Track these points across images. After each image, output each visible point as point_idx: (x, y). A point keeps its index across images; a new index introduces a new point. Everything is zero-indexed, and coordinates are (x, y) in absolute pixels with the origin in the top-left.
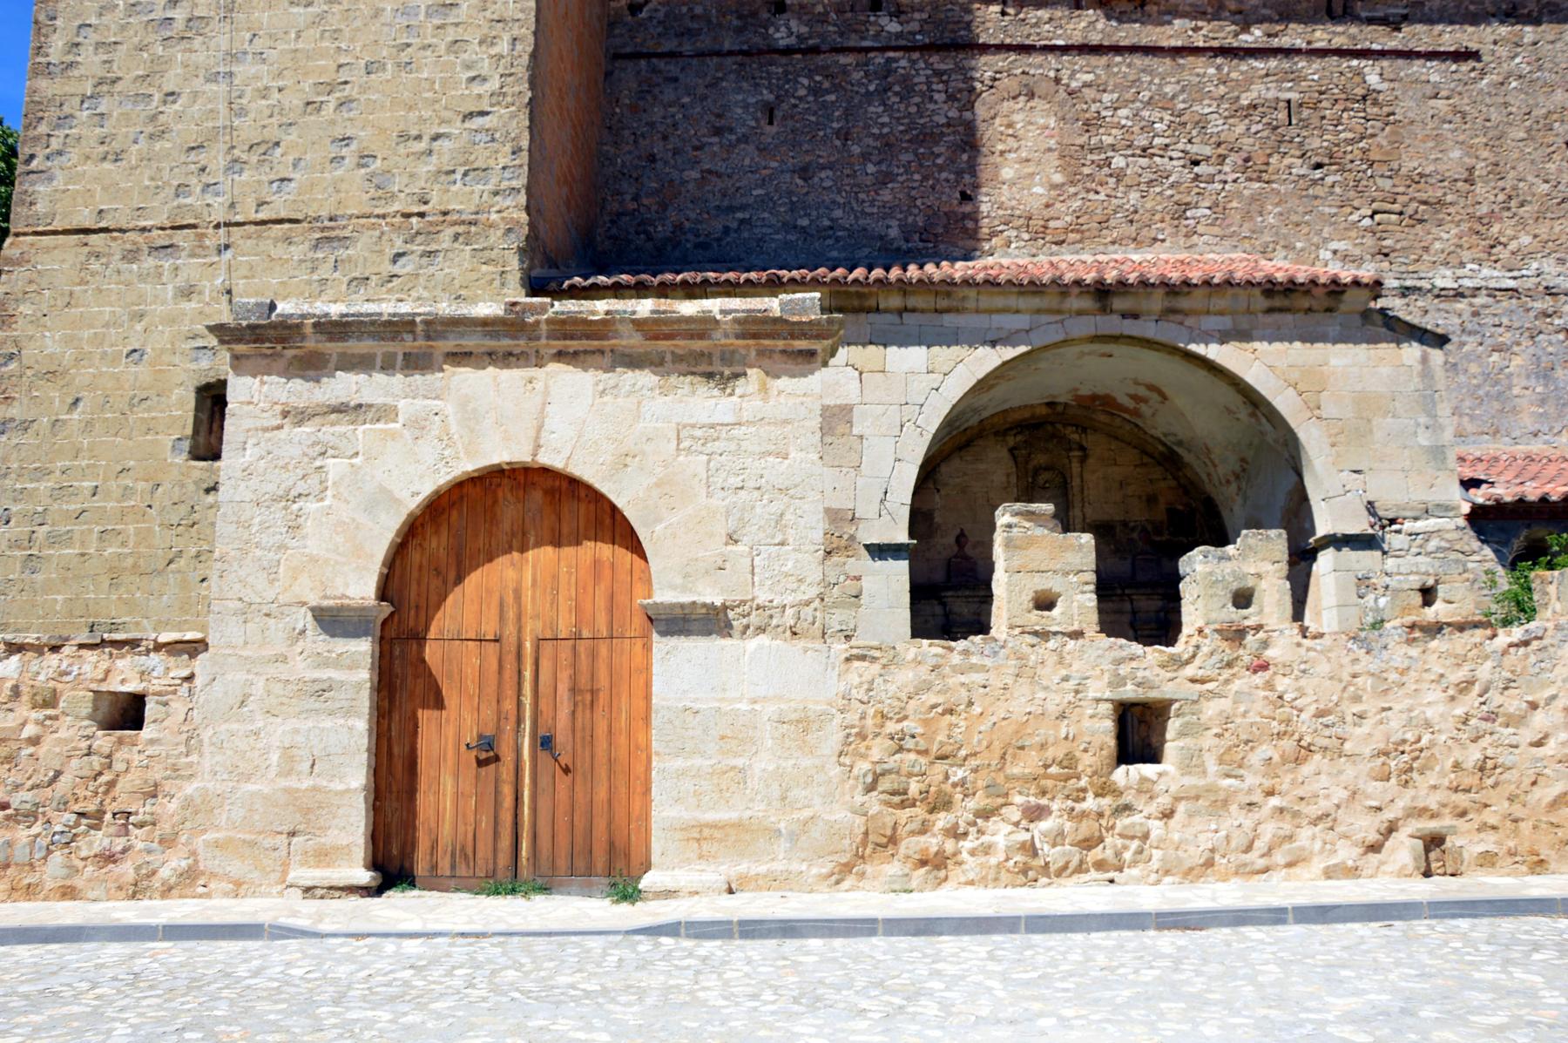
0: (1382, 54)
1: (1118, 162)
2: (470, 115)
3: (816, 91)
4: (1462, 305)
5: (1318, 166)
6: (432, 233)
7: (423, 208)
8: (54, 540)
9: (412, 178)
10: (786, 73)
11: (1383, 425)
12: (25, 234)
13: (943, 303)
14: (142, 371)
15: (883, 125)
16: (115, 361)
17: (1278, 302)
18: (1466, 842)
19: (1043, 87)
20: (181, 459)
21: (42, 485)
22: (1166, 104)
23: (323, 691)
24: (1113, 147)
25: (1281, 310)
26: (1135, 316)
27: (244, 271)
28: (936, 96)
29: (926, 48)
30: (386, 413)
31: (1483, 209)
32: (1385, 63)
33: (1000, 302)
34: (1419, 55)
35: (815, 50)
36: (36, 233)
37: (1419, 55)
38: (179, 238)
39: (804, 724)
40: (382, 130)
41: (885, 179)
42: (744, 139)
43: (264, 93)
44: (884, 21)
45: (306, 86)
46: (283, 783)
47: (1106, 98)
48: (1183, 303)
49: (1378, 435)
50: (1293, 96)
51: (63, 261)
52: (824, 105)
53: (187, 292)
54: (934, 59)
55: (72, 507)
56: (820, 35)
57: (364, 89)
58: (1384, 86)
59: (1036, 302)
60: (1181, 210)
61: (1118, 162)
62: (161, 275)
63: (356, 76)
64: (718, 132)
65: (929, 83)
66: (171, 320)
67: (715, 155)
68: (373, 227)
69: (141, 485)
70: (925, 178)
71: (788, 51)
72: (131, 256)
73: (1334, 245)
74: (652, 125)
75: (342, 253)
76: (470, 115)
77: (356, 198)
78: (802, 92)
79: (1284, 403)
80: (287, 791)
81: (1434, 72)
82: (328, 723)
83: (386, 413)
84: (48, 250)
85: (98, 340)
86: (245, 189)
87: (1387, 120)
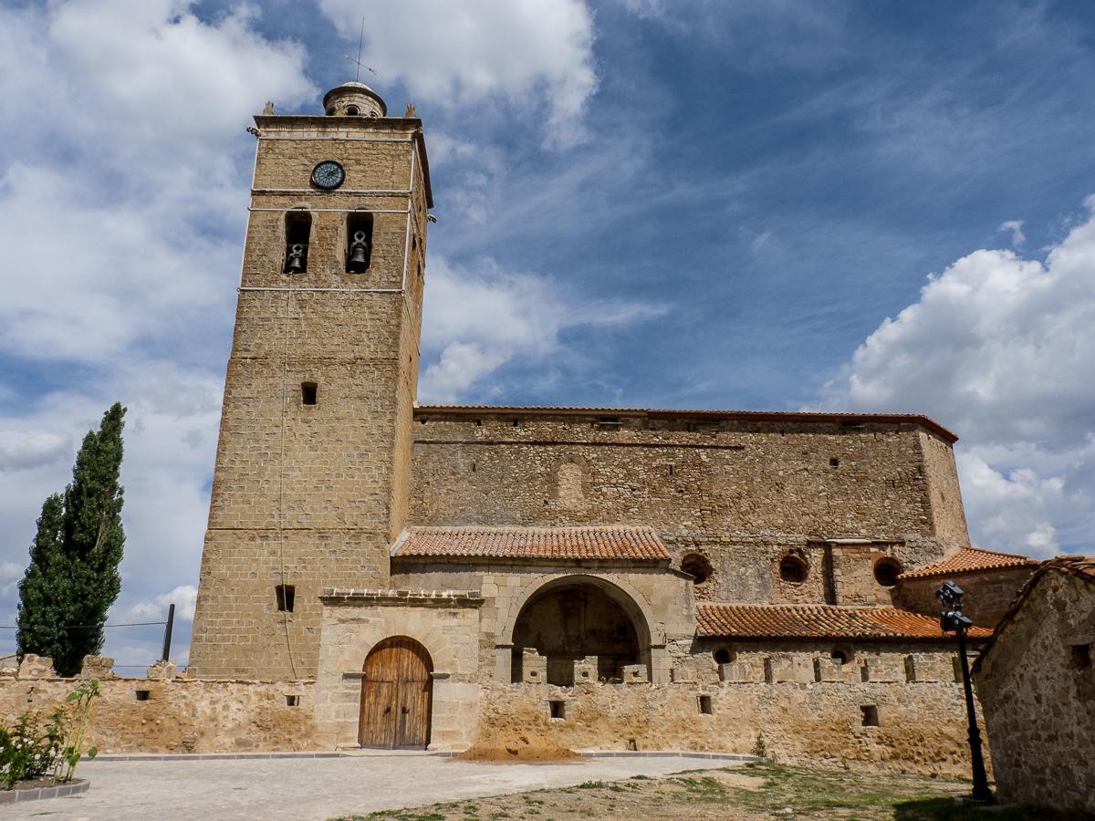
0: (708, 447)
1: (604, 490)
2: (372, 494)
3: (491, 459)
4: (731, 548)
5: (681, 491)
6: (356, 536)
7: (355, 527)
8: (224, 639)
10: (480, 450)
11: (671, 607)
13: (526, 563)
15: (517, 473)
17: (637, 565)
18: (639, 742)
21: (218, 620)
22: (624, 466)
23: (348, 695)
24: (603, 484)
25: (639, 567)
26: (589, 568)
28: (537, 462)
29: (535, 443)
30: (367, 621)
31: (743, 509)
32: (708, 450)
33: (545, 563)
34: (722, 448)
35: (491, 443)
37: (722, 448)
39: (471, 705)
41: (516, 494)
42: (463, 478)
43: (299, 482)
44: (518, 431)
45: (314, 480)
46: (337, 720)
48: (605, 565)
49: (669, 611)
50: (673, 463)
52: (495, 464)
53: (273, 553)
56: (495, 436)
59: (556, 564)
60: (626, 509)
61: (604, 490)
63: (334, 479)
64: (453, 474)
65: (534, 456)
66: (266, 562)
67: (452, 483)
68: (338, 533)
69: (254, 621)
70: (531, 495)
71: (481, 443)
72: (253, 539)
73: (685, 523)
74: (428, 470)
75: (327, 542)
76: (372, 494)
77: (334, 523)
78: (486, 458)
79: (638, 599)
80: (338, 722)
81: (726, 454)
82: (349, 704)
83: (367, 621)
84: (221, 536)
85: (239, 569)
86: (291, 517)
87: (709, 473)
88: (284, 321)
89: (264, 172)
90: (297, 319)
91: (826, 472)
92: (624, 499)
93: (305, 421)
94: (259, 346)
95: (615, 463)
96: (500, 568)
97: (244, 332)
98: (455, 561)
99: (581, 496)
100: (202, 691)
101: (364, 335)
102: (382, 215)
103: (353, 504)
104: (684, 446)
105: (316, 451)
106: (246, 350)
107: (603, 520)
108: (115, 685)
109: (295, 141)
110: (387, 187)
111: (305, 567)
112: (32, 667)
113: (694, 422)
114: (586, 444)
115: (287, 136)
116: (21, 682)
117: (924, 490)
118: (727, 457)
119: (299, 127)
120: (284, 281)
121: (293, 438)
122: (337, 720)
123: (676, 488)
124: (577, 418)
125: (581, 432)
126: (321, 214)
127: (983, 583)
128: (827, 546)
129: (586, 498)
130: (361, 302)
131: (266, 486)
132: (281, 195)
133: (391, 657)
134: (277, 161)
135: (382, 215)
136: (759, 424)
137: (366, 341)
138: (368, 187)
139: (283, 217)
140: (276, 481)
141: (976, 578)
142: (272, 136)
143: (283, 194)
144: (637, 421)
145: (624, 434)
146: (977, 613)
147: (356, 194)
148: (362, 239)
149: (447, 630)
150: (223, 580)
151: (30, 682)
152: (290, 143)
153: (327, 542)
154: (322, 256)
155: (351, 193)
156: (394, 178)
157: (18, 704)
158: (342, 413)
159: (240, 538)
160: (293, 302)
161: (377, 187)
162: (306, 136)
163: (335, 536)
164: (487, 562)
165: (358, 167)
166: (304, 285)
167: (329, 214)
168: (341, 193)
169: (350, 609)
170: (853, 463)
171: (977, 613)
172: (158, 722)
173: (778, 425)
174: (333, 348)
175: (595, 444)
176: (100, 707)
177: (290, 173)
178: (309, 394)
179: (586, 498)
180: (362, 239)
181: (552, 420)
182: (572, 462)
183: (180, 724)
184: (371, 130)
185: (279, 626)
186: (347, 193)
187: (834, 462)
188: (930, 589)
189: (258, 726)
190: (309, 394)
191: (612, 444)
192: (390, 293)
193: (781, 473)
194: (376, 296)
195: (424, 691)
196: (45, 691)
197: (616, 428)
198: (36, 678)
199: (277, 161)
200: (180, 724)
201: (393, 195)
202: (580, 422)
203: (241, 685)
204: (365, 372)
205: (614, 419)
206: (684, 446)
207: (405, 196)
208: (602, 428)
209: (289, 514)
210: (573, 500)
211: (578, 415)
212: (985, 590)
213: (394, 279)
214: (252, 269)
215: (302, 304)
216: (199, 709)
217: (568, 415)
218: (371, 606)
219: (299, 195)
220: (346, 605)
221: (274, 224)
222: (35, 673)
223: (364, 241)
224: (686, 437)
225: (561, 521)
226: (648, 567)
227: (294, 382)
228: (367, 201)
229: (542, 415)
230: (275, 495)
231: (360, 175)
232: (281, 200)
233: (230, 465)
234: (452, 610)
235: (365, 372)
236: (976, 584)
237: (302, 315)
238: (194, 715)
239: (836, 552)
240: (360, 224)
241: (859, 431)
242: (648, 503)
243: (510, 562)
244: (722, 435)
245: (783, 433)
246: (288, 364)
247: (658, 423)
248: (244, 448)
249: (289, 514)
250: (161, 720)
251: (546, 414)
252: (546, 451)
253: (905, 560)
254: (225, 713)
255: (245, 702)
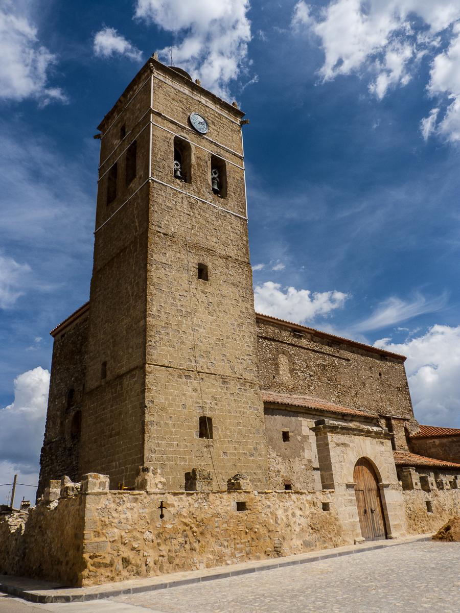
7: (241, 377)
8: (168, 459)
9: (239, 368)
12: (151, 364)
13: (321, 414)
14: (186, 411)
16: (179, 407)
19: (286, 353)
20: (197, 438)
22: (305, 361)
27: (207, 386)
36: (154, 365)
38: (191, 373)
40: (231, 355)
45: (214, 338)
46: (350, 520)
47: (296, 357)
50: (325, 363)
51: (162, 375)
53: (195, 390)
54: (266, 341)
55: (171, 449)
57: (227, 343)
58: (338, 364)
60: (309, 387)
62: (187, 383)
63: (225, 339)
68: (233, 380)
69: (188, 444)
72: (180, 376)
73: (333, 399)
75: (228, 386)
77: (228, 372)
80: (350, 522)
81: (344, 362)
84: (159, 371)
85: (174, 400)
88: (182, 214)
89: (158, 101)
90: (190, 215)
91: (378, 379)
92: (308, 381)
93: (203, 292)
94: (167, 226)
95: (302, 358)
96: (309, 415)
97: (156, 211)
98: (289, 409)
99: (289, 376)
100: (278, 501)
101: (230, 241)
102: (230, 165)
103: (239, 361)
104: (328, 355)
105: (212, 316)
106: (159, 226)
107: (300, 393)
108: (223, 498)
109: (175, 89)
110: (231, 148)
111: (216, 404)
112: (157, 481)
113: (330, 342)
114: (288, 344)
115: (170, 83)
116: (152, 496)
117: (408, 394)
118: (344, 364)
119: (177, 81)
120: (179, 185)
121: (197, 303)
122: (350, 520)
123: (328, 377)
124: (283, 327)
125: (285, 335)
126: (196, 147)
127: (454, 442)
128: (388, 420)
129: (292, 377)
130: (225, 218)
131: (184, 336)
132: (171, 122)
133: (359, 473)
134: (166, 97)
135: (230, 165)
136: (354, 349)
137: (231, 247)
138: (221, 143)
139: (173, 138)
140: (190, 334)
141: (450, 439)
142: (161, 78)
143: (172, 122)
144: (309, 336)
145: (304, 342)
146: (451, 456)
147: (215, 144)
148: (217, 175)
149: (382, 453)
150: (163, 409)
151: (159, 496)
152: (172, 90)
153: (228, 386)
154: (200, 177)
155: (212, 142)
156: (234, 144)
157: (152, 520)
158: (225, 292)
159: (171, 375)
160: (186, 203)
161: (226, 145)
162: (182, 89)
163: (232, 383)
164: (303, 411)
165: (213, 127)
166: (189, 191)
167: (200, 151)
168: (207, 139)
169: (339, 436)
170: (386, 376)
171: (451, 456)
172: (256, 530)
173: (360, 351)
174: (213, 244)
175: (292, 345)
176: (216, 519)
177: (175, 110)
178: (202, 273)
179: (292, 377)
180: (217, 175)
181: (273, 326)
182: (284, 354)
183: (269, 531)
184: (218, 107)
185: (205, 450)
186: (210, 141)
187: (380, 375)
188: (427, 444)
189: (312, 529)
190: (202, 273)
191: (300, 347)
192: (240, 218)
193: (364, 377)
194: (233, 217)
195: (377, 497)
196: (173, 506)
197: (300, 337)
198: (164, 492)
199: (166, 97)
200: (269, 531)
201: (235, 155)
202: (285, 330)
203: (297, 495)
204: (234, 267)
205: (300, 331)
206: (328, 355)
207: (240, 158)
208: (295, 336)
209: (201, 360)
210: (286, 378)
211: (284, 326)
212: (454, 445)
213: (241, 210)
214: (157, 167)
215: (191, 206)
216: (279, 517)
217: (280, 325)
218: (349, 435)
219: (184, 128)
220: (337, 433)
221: (168, 140)
222: (160, 486)
223: (218, 177)
224: (327, 349)
225: (282, 390)
226: (368, 422)
227: (192, 261)
228: (222, 152)
229: (268, 321)
230: (189, 344)
231: (216, 133)
232: (171, 125)
233: (157, 314)
234: (381, 440)
235: (234, 267)
236: (450, 442)
237: (192, 214)
238: (276, 522)
239: (393, 422)
240: (218, 165)
241: (386, 360)
242: (318, 385)
243: (314, 413)
244: (342, 352)
245: (362, 355)
246: (190, 247)
247: (317, 339)
248: (166, 302)
249: (201, 360)
250: (258, 529)
251: (270, 322)
252: (271, 345)
253: (410, 429)
254: (294, 519)
255: (303, 509)
